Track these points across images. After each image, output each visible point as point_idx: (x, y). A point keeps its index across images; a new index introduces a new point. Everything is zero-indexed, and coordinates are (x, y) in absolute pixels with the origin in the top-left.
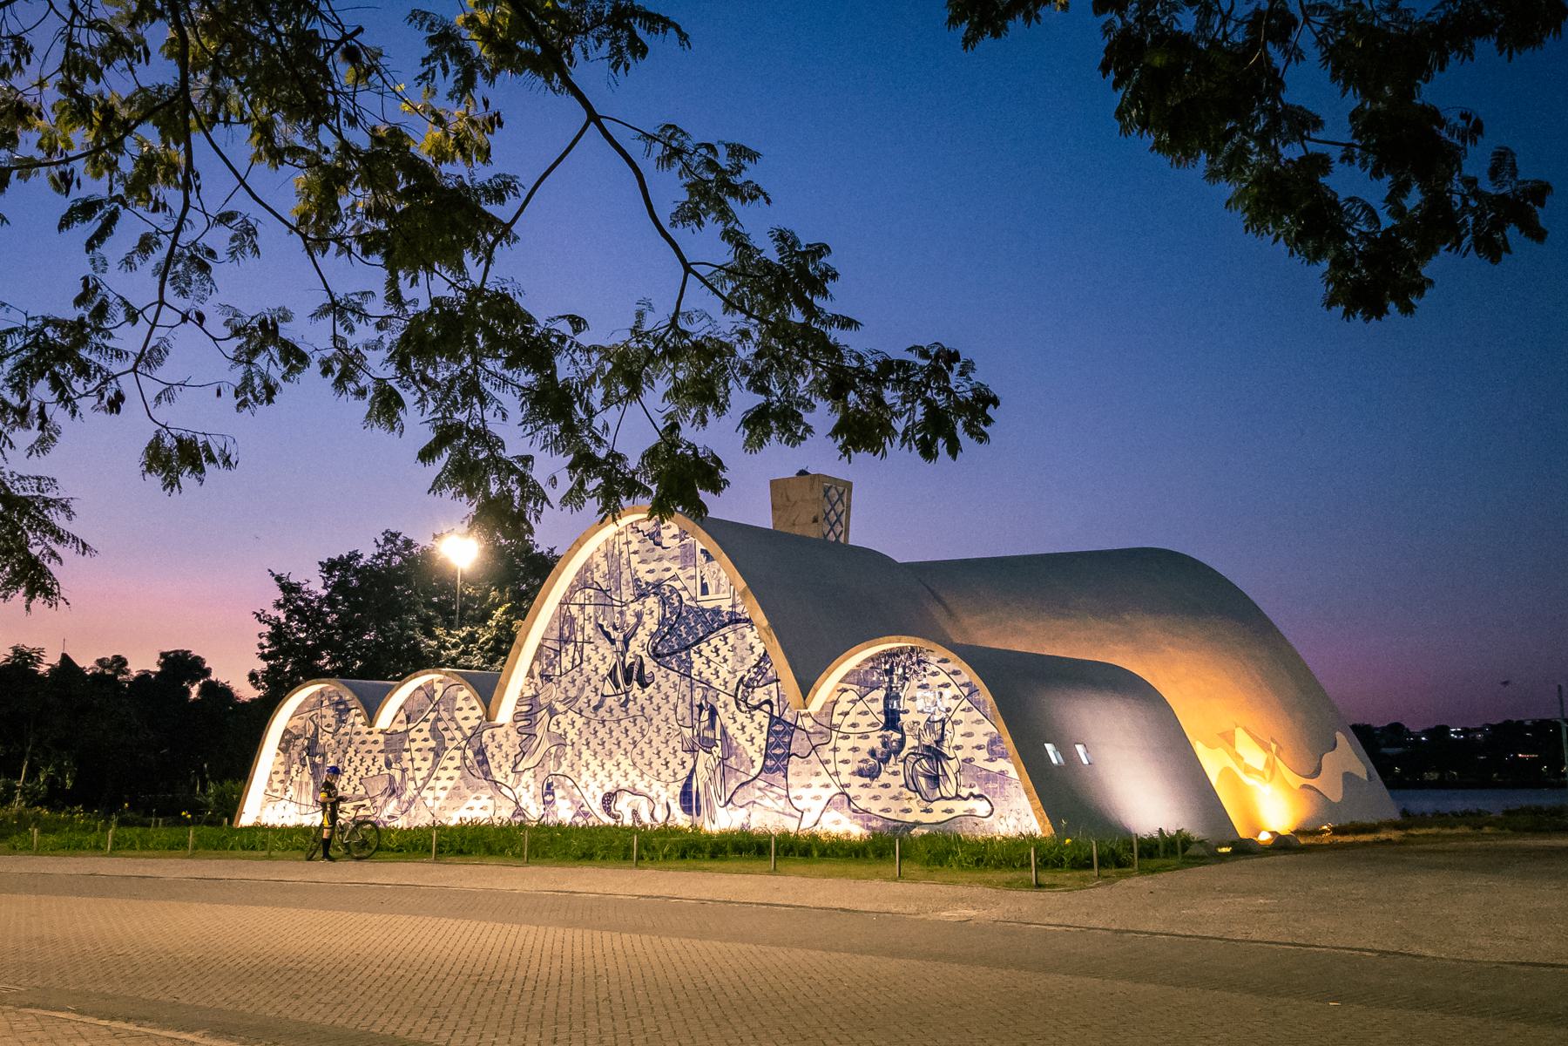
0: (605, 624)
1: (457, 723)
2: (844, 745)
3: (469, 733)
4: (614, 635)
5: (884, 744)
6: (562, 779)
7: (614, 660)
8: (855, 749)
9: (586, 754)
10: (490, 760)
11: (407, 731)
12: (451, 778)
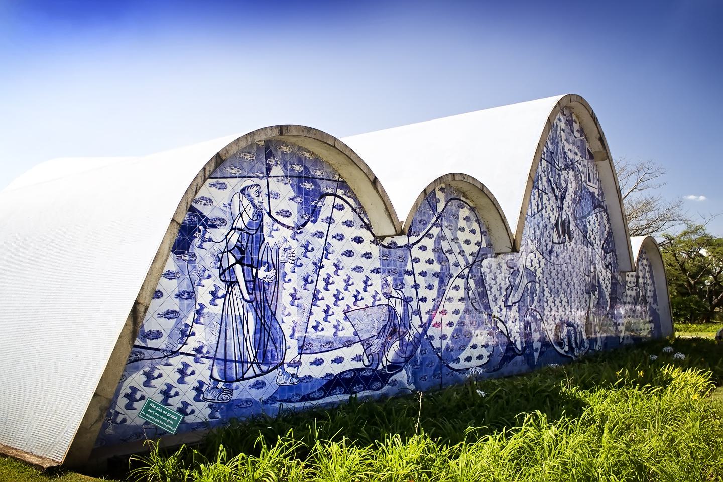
0: (552, 180)
1: (460, 246)
2: (629, 292)
3: (471, 259)
4: (557, 192)
5: (636, 293)
6: (535, 313)
7: (558, 214)
8: (630, 296)
9: (547, 290)
10: (488, 293)
11: (409, 246)
12: (456, 312)
